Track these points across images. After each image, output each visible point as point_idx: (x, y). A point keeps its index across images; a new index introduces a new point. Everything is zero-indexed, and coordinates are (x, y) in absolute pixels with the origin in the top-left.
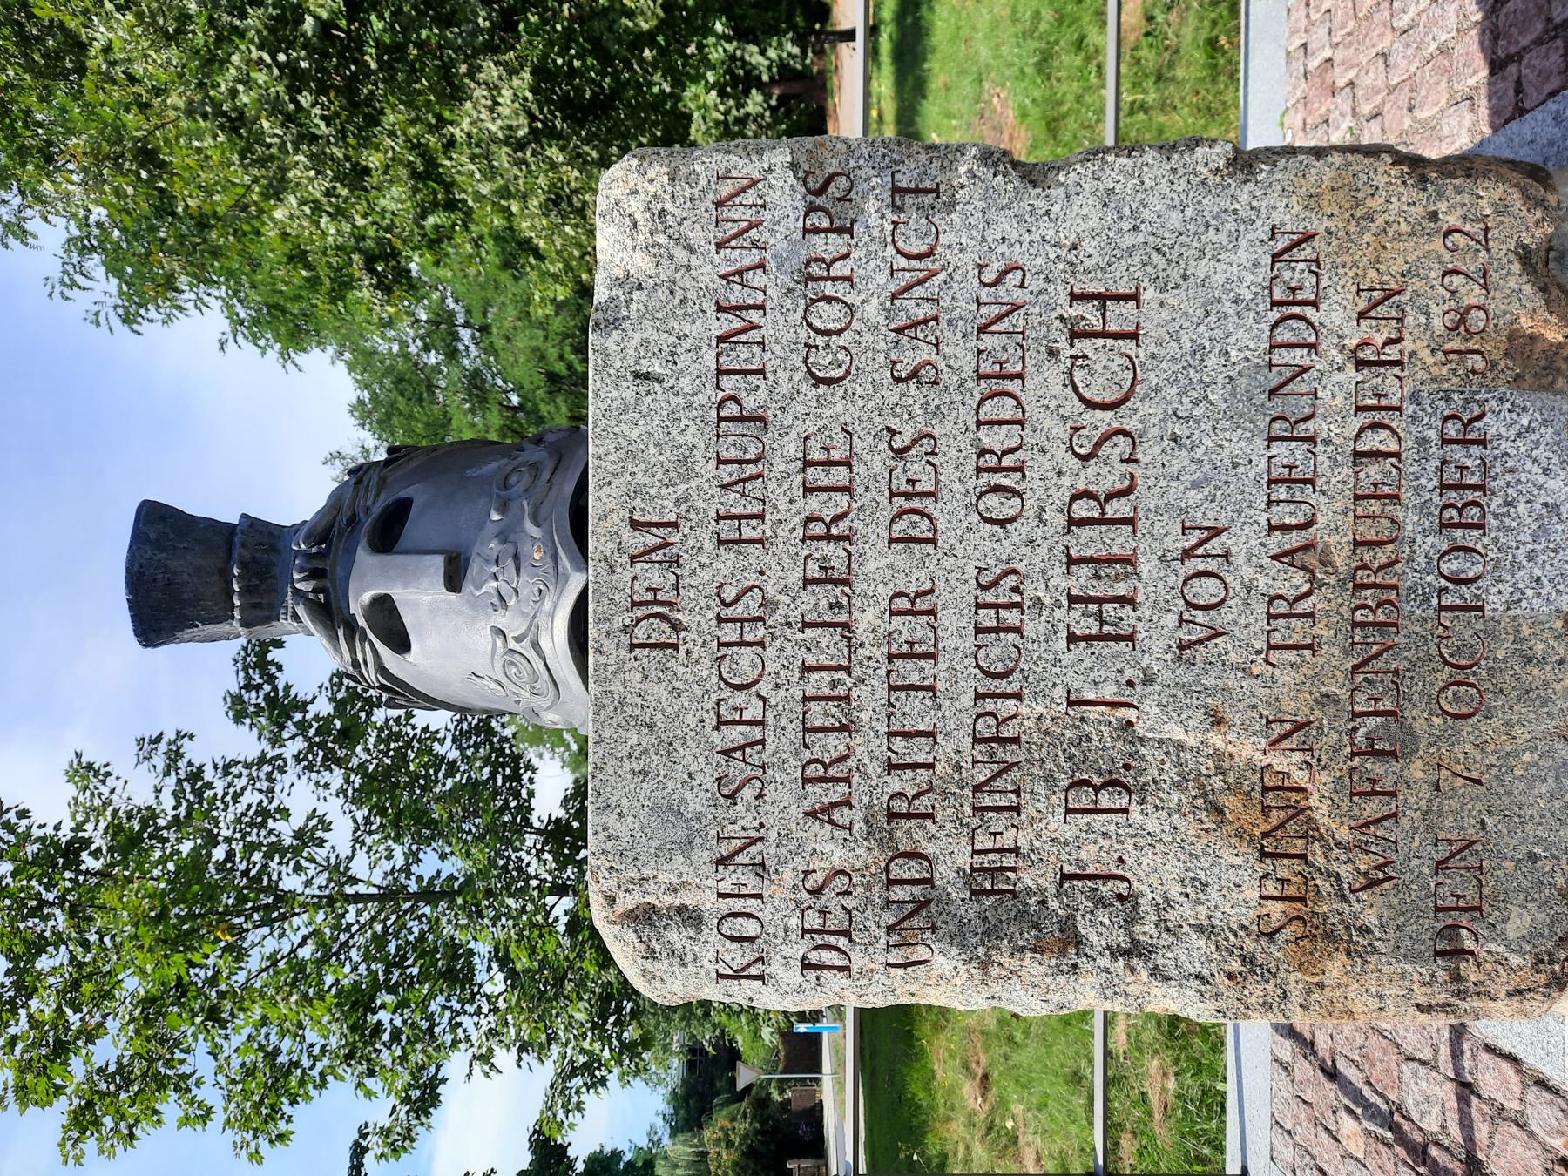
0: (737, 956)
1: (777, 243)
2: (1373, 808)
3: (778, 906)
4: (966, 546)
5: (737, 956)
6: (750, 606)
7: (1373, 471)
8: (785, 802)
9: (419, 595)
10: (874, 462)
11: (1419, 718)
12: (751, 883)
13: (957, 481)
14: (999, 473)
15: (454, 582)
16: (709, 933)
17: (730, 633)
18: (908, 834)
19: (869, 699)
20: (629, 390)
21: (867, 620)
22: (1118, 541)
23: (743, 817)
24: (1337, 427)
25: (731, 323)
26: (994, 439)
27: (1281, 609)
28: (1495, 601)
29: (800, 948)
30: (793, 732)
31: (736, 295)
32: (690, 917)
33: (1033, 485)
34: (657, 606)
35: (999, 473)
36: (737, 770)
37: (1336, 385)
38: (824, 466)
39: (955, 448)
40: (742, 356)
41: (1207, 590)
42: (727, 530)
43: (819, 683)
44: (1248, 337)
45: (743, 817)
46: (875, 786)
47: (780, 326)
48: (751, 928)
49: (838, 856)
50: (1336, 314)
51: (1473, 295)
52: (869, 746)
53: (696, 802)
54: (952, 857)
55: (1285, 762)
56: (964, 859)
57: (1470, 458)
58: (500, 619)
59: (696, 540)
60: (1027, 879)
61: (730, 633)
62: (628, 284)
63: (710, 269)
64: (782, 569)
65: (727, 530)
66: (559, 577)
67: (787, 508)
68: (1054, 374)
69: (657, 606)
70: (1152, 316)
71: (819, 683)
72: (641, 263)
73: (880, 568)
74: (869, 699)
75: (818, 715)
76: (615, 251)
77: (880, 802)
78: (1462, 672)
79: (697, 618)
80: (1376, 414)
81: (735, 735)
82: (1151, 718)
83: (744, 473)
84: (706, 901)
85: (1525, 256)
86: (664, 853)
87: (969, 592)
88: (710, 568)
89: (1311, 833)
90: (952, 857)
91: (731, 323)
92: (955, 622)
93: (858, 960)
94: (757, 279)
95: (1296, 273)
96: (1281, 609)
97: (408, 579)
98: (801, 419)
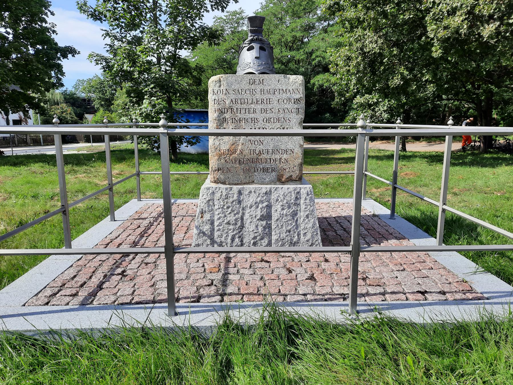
0: (216, 92)
1: (293, 95)
2: (234, 161)
3: (221, 96)
4: (260, 116)
5: (216, 92)
6: (254, 93)
7: (269, 160)
8: (233, 97)
9: (254, 53)
10: (270, 106)
11: (243, 165)
12: (224, 93)
13: (268, 116)
14: (268, 120)
15: (256, 58)
16: (218, 88)
17: (251, 90)
18: (230, 110)
19: (245, 106)
20: (277, 79)
21: (253, 106)
23: (231, 92)
24: (273, 157)
26: (272, 120)
27: (254, 151)
28: (255, 174)
29: (217, 98)
30: (240, 97)
31: (287, 91)
32: (220, 86)
33: (267, 124)
34: (254, 82)
35: (268, 120)
36: (236, 91)
37: (278, 157)
38: (269, 101)
39: (271, 115)
40: (281, 92)
41: (256, 143)
42: (262, 90)
43: (246, 101)
44: (283, 147)
45: (231, 92)
46: (235, 107)
47: (284, 96)
48: (219, 93)
49: (227, 103)
50: (285, 156)
51: (287, 170)
52: (239, 106)
53: (233, 87)
54: (227, 116)
55: (238, 152)
56: (227, 117)
57: (270, 170)
58: (252, 64)
59: (261, 87)
60: (225, 124)
61: (251, 90)
62: (289, 78)
63: (290, 88)
64: (258, 96)
65: (262, 90)
66: (257, 71)
67: (265, 97)
69: (254, 82)
71: (246, 101)
72: (291, 80)
73: (259, 107)
74: (245, 106)
75: (243, 100)
77: (233, 107)
78: (249, 170)
79: (253, 87)
80: (275, 160)
81: (240, 91)
83: (269, 92)
84: (222, 88)
85: (291, 176)
86: (228, 83)
87: (256, 117)
88: (258, 88)
89: (231, 155)
90: (227, 116)
92: (252, 116)
93: (216, 105)
94: (289, 93)
95: (289, 152)
96: (254, 151)
97: (256, 52)
98: (274, 99)
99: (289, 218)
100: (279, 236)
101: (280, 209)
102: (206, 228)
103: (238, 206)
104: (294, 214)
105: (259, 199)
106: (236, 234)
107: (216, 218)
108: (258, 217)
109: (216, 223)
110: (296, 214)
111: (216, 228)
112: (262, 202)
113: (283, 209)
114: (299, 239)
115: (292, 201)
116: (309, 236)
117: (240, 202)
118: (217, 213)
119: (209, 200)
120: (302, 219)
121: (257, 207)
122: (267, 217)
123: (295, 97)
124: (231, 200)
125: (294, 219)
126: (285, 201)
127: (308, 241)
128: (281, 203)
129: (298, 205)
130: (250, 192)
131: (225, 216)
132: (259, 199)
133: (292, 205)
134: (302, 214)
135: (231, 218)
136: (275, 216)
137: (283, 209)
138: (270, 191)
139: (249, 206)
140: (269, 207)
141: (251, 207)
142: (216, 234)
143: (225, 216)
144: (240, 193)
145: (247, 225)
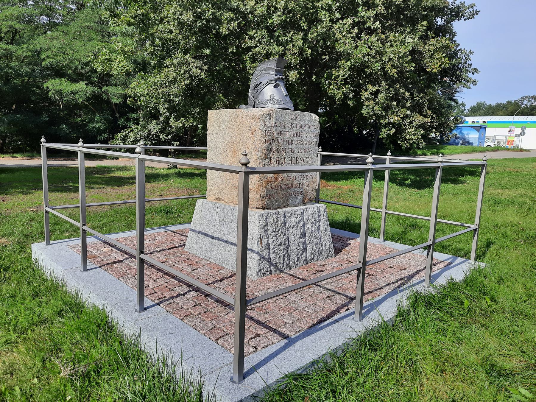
4: (295, 147)
8: (279, 129)
14: (300, 151)
19: (286, 138)
22: (295, 162)
54: (274, 146)
63: (313, 124)
64: (295, 130)
73: (294, 139)
74: (286, 138)
80: (302, 185)
90: (274, 146)
92: (290, 147)
101: (310, 227)
102: (265, 252)
105: (298, 219)
106: (285, 255)
107: (271, 241)
108: (299, 236)
109: (271, 247)
111: (272, 251)
112: (300, 221)
116: (327, 246)
117: (285, 224)
118: (271, 237)
121: (297, 226)
122: (303, 235)
126: (313, 219)
129: (319, 221)
130: (291, 214)
132: (298, 219)
135: (281, 240)
136: (308, 234)
137: (312, 226)
139: (292, 226)
142: (272, 256)
145: (291, 245)
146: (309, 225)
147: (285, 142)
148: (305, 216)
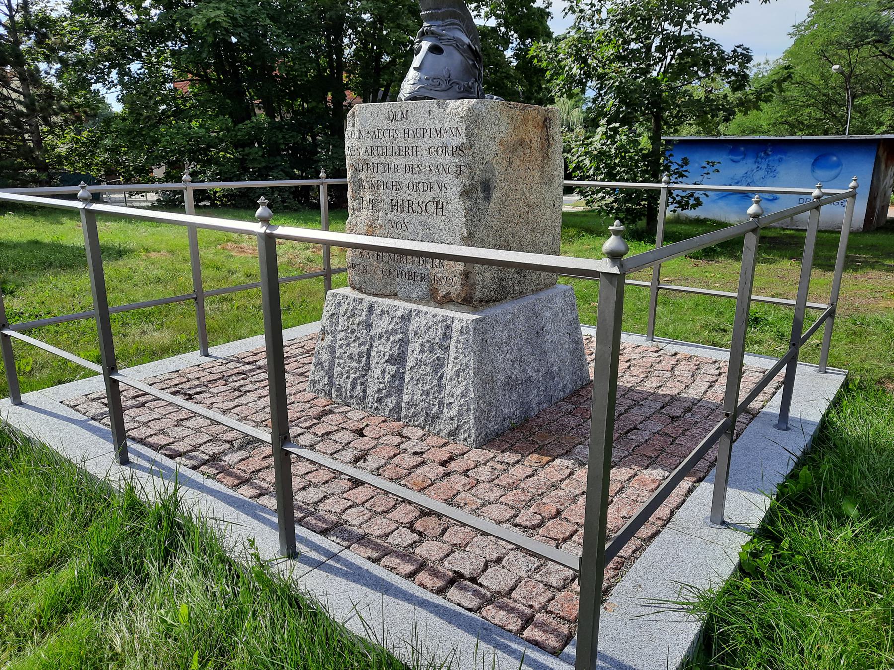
1: (451, 140)
4: (405, 178)
8: (368, 143)
14: (415, 186)
19: (382, 160)
20: (427, 109)
22: (406, 210)
25: (438, 130)
28: (399, 281)
30: (377, 144)
36: (372, 133)
45: (366, 135)
57: (418, 278)
63: (446, 126)
64: (401, 142)
68: (430, 198)
70: (440, 218)
73: (401, 161)
75: (380, 149)
76: (453, 104)
78: (389, 273)
79: (393, 125)
82: (382, 214)
83: (415, 134)
85: (449, 293)
87: (398, 180)
88: (400, 126)
91: (438, 130)
92: (393, 177)
99: (429, 369)
100: (412, 398)
101: (417, 351)
103: (365, 331)
104: (438, 365)
105: (391, 326)
106: (358, 378)
107: (339, 343)
108: (386, 358)
110: (442, 365)
112: (395, 332)
113: (422, 352)
114: (441, 411)
115: (437, 340)
116: (454, 412)
117: (369, 326)
119: (333, 315)
120: (449, 376)
122: (398, 359)
123: (454, 144)
124: (356, 321)
125: (436, 373)
127: (452, 419)
128: (420, 341)
131: (348, 345)
132: (391, 326)
133: (436, 348)
134: (450, 367)
135: (354, 350)
136: (411, 361)
138: (409, 315)
140: (404, 342)
141: (380, 338)
142: (337, 370)
143: (348, 345)
144: (370, 309)
145: (373, 367)
146: (414, 346)
147: (381, 169)
148: (412, 326)
